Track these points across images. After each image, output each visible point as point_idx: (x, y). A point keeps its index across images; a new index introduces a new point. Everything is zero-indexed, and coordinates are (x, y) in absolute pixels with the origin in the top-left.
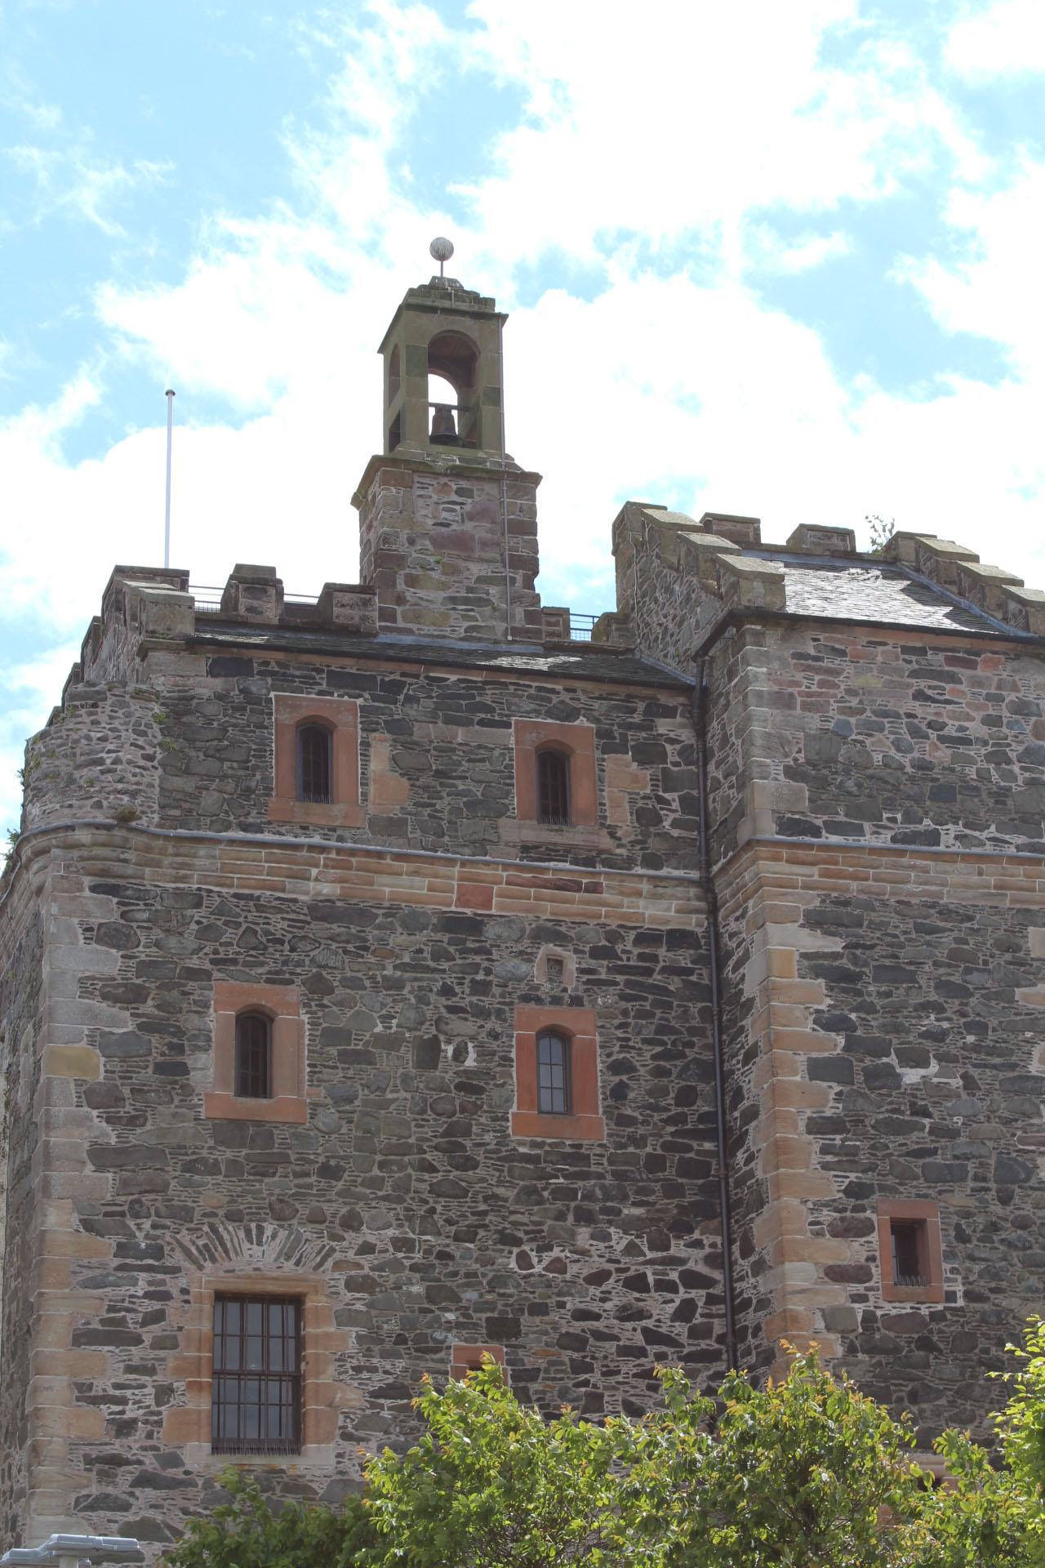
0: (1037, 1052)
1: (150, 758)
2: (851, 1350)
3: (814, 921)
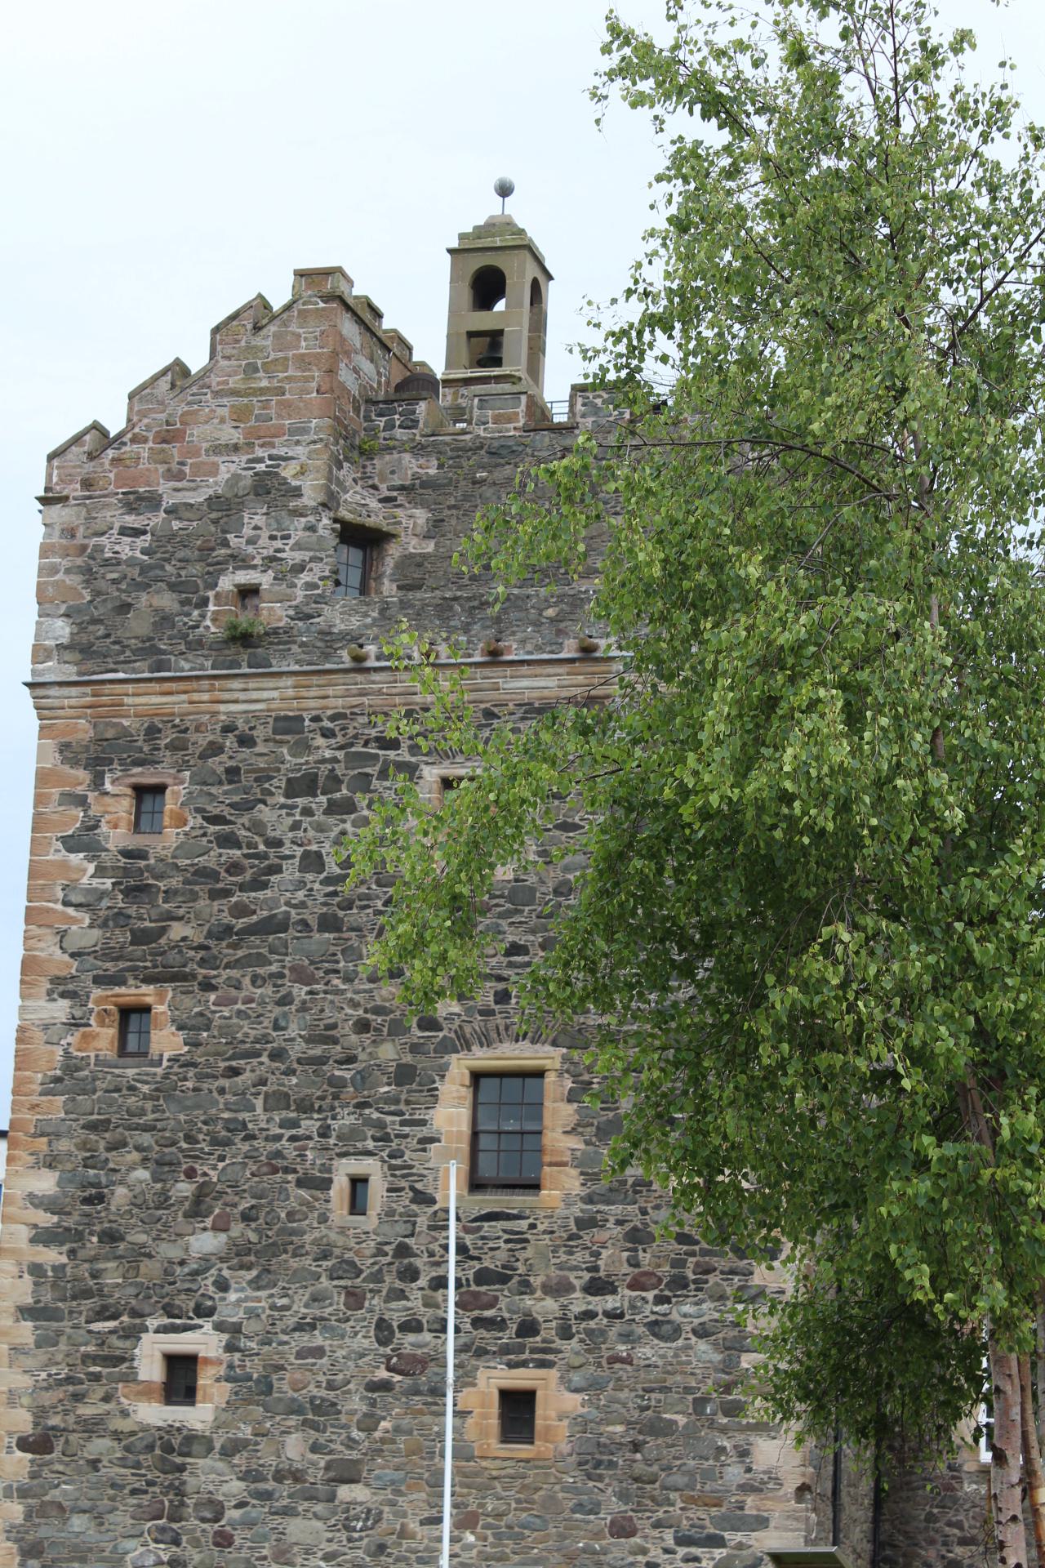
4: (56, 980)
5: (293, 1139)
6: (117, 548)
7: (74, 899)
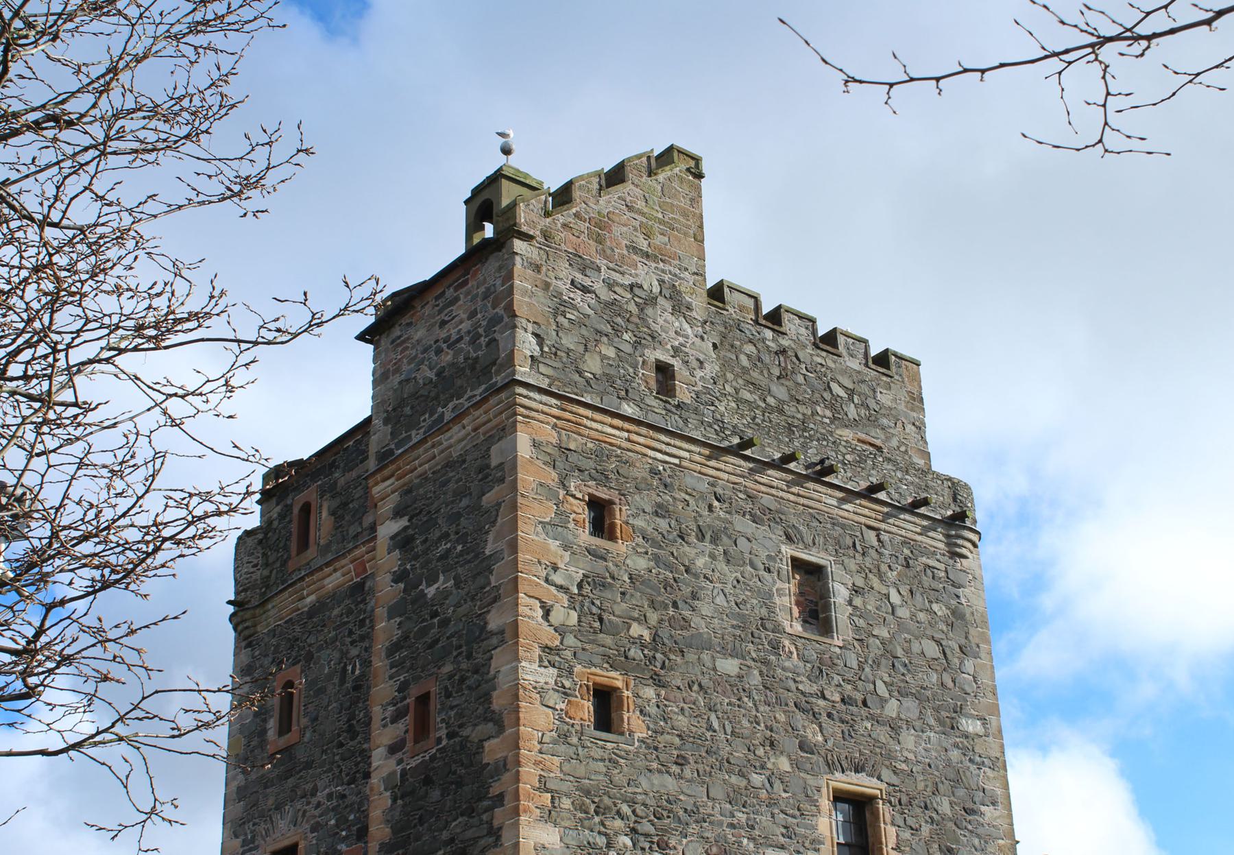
0: (491, 537)
1: (255, 566)
2: (394, 800)
3: (397, 513)
4: (547, 649)
5: (732, 826)
6: (572, 295)
7: (558, 578)
